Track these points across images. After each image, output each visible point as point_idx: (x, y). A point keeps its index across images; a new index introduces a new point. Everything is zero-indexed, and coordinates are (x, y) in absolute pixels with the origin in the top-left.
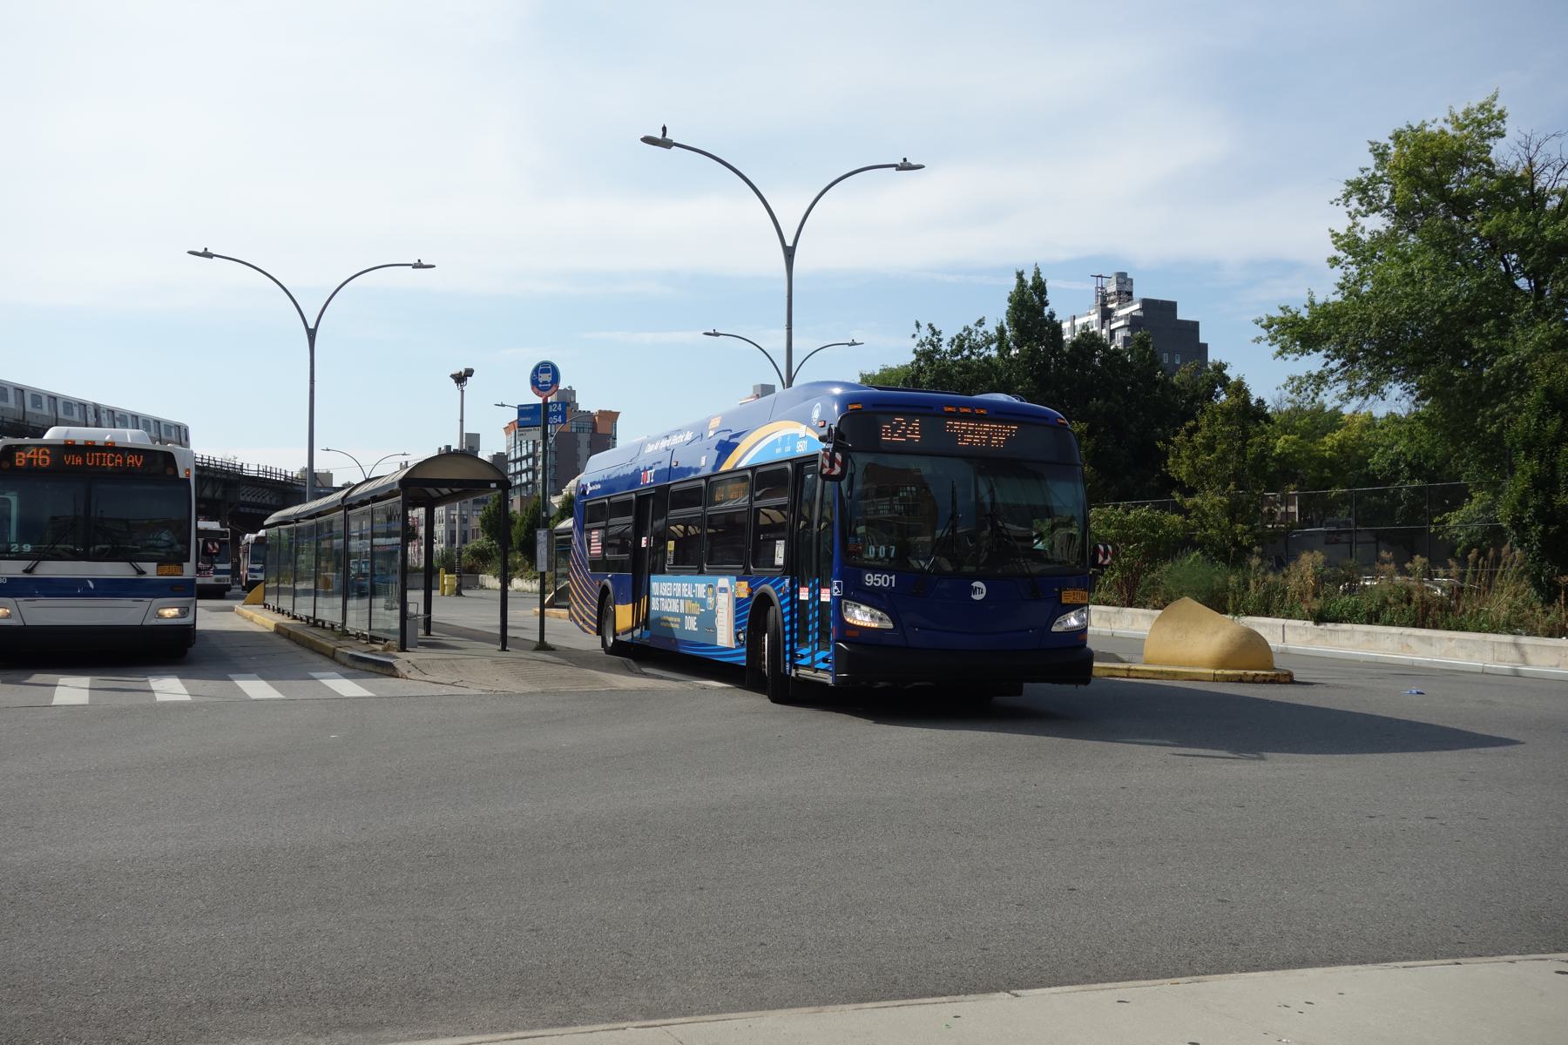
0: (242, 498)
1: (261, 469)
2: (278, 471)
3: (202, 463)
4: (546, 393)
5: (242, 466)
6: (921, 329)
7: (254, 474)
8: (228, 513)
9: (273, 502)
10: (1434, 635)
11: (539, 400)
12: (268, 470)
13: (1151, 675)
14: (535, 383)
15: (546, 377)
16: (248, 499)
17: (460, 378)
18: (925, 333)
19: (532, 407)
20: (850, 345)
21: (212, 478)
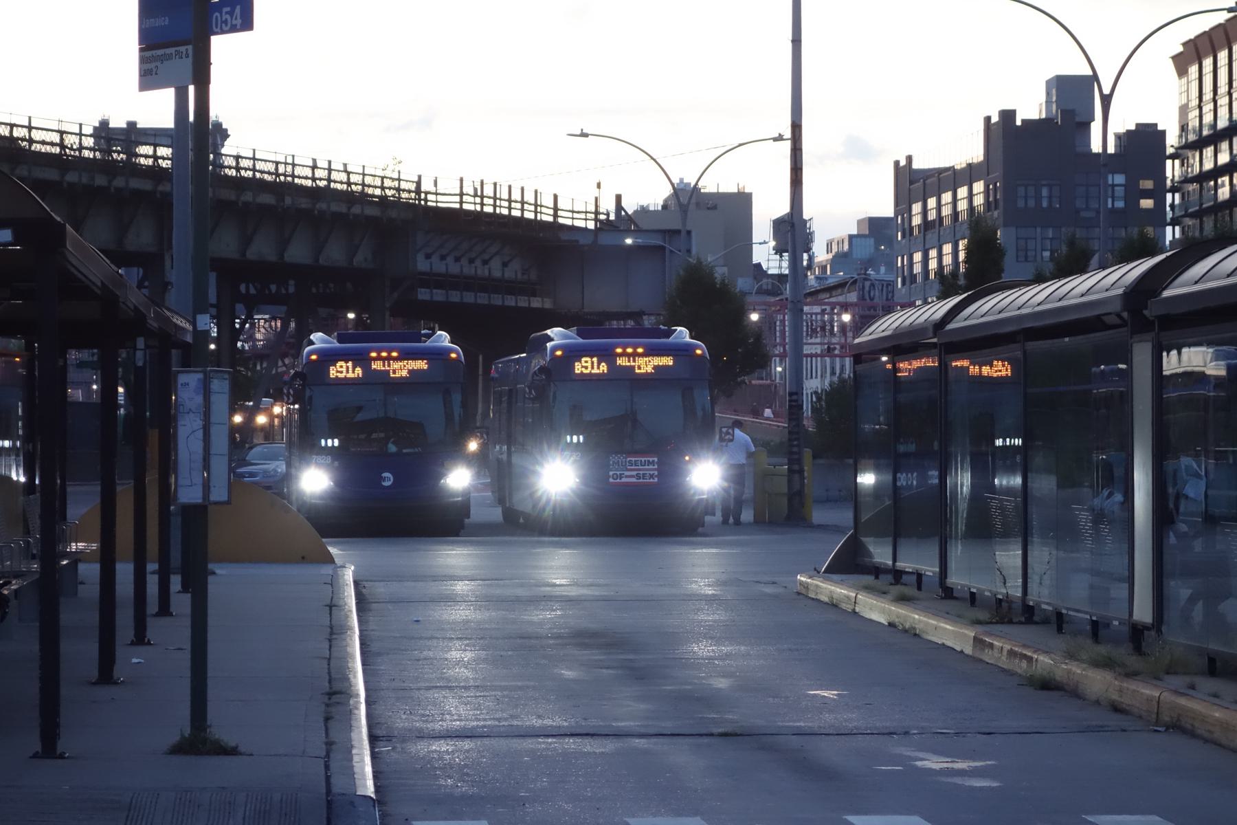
0: (422, 265)
1: (468, 189)
2: (516, 195)
3: (314, 179)
5: (419, 183)
7: (451, 203)
8: (388, 305)
9: (509, 274)
16: (439, 267)
21: (337, 216)
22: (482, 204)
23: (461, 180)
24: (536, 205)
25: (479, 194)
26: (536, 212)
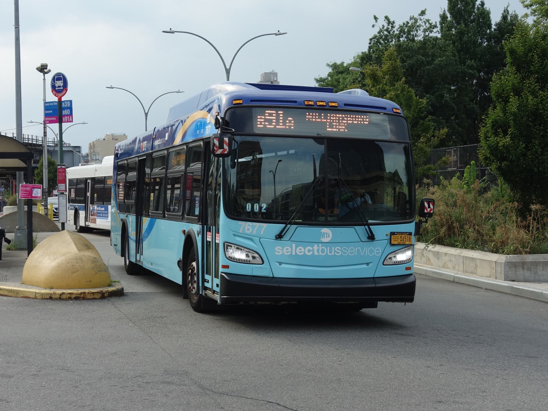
2: (30, 137)
6: (378, 21)
10: (449, 252)
13: (6, 293)
18: (382, 22)
20: (276, 35)
24: (36, 140)
26: (36, 142)
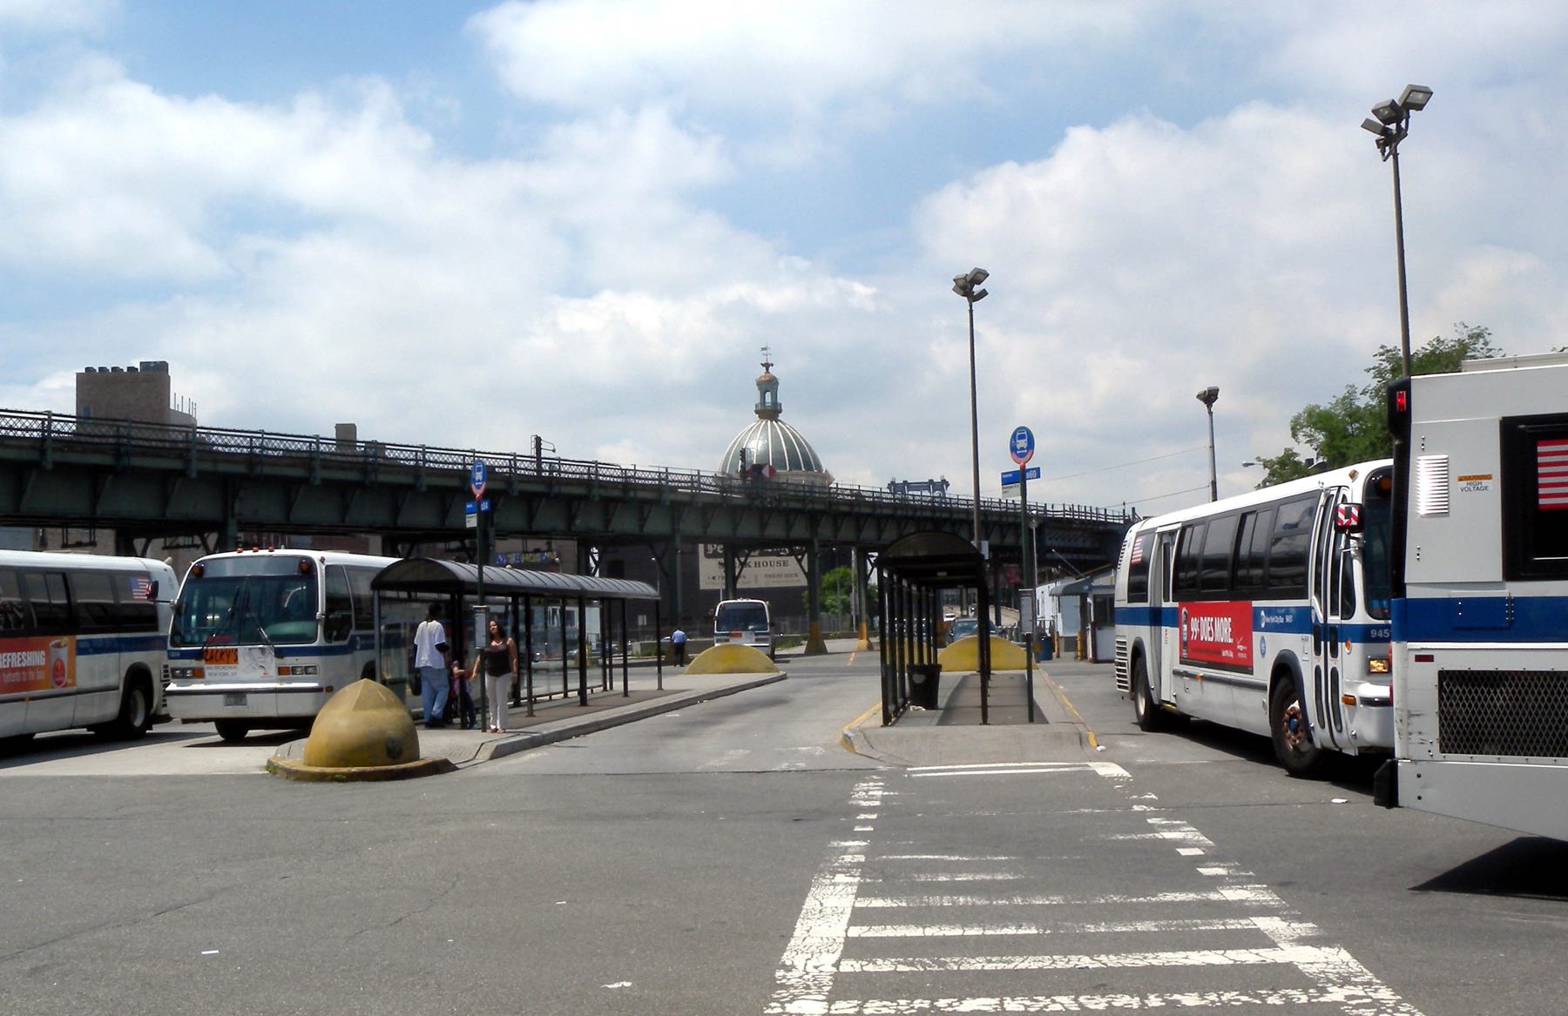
2: (1088, 510)
3: (1000, 508)
4: (1023, 460)
7: (1060, 515)
11: (1017, 468)
12: (1088, 510)
14: (1013, 449)
15: (1022, 443)
17: (1209, 397)
19: (1011, 475)
22: (1073, 515)
23: (1064, 505)
25: (1071, 510)
